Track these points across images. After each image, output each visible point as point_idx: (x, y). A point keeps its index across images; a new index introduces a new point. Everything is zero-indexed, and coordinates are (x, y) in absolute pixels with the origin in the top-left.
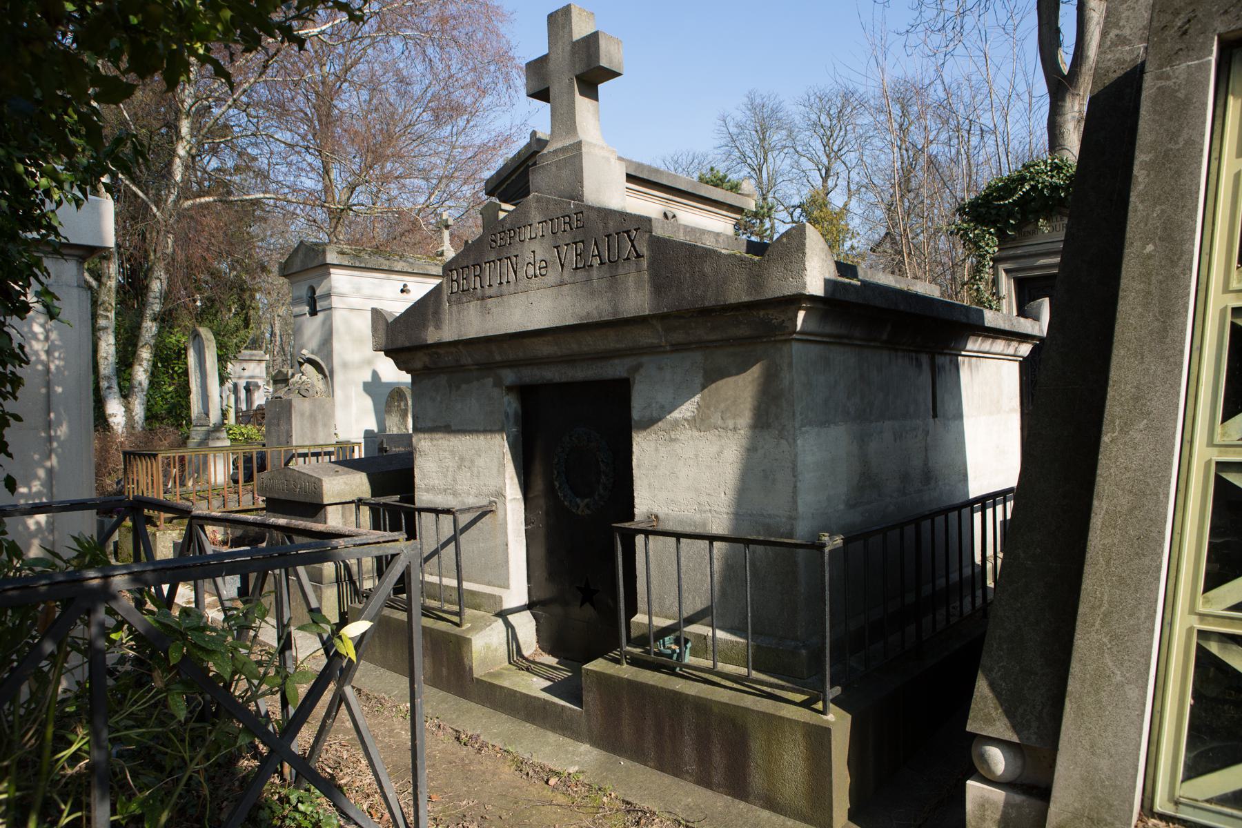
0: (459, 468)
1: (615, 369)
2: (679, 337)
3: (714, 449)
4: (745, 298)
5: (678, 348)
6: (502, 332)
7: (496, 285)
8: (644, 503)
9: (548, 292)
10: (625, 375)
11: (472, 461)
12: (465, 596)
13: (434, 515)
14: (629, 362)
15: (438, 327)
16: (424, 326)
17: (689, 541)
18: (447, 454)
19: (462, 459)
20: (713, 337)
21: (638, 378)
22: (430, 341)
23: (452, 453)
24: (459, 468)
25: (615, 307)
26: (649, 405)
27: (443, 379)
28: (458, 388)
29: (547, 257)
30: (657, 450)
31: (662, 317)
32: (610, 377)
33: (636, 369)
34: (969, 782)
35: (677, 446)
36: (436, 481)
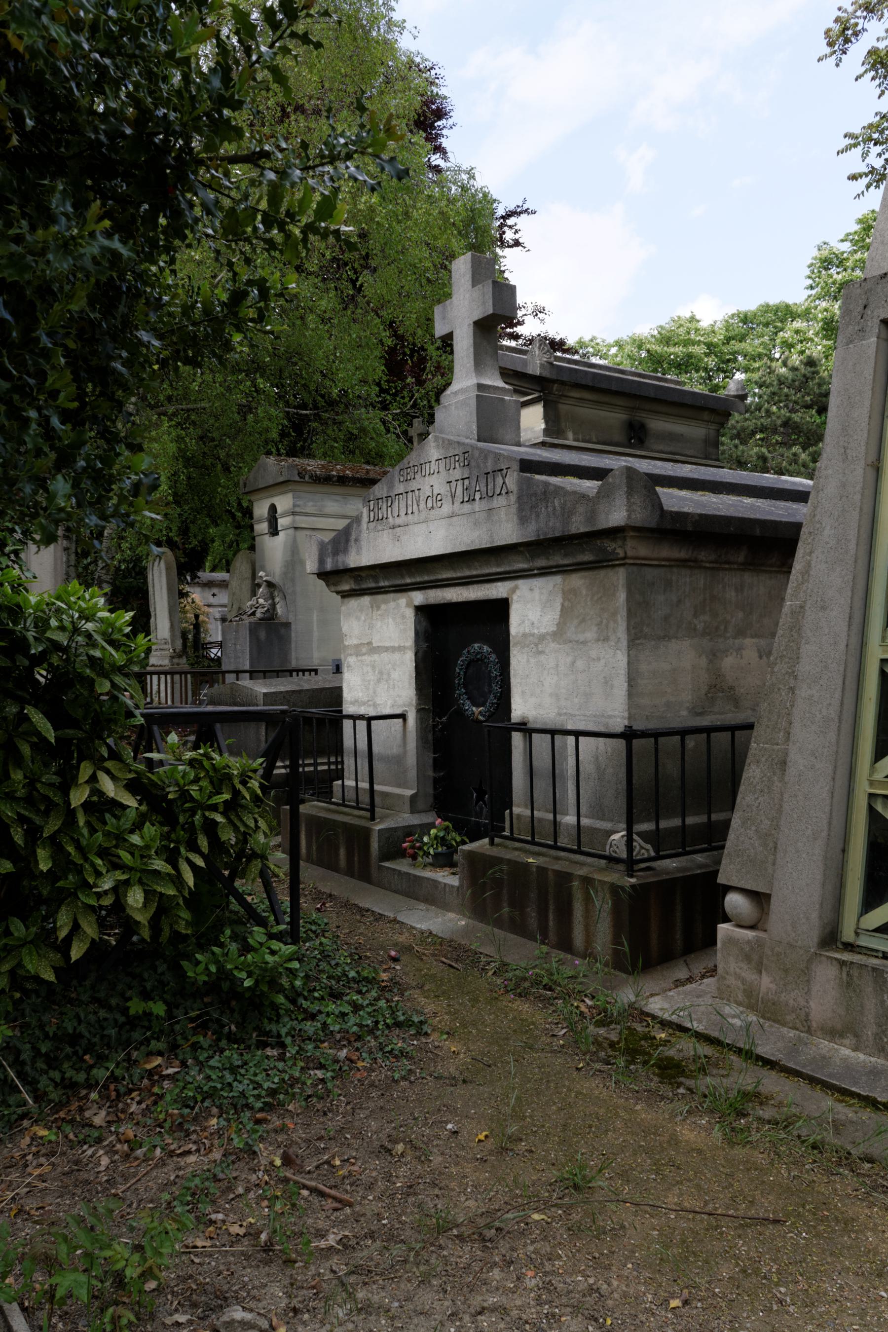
0: (379, 681)
1: (497, 591)
2: (541, 562)
3: (569, 659)
4: (582, 530)
5: (545, 572)
6: (408, 558)
7: (402, 513)
8: (521, 707)
9: (444, 522)
10: (504, 595)
11: (389, 674)
12: (377, 800)
13: (549, 736)
14: (509, 585)
15: (359, 551)
16: (346, 551)
17: (588, 738)
18: (369, 669)
19: (381, 673)
20: (566, 562)
21: (515, 597)
22: (352, 565)
23: (373, 667)
24: (379, 681)
25: (491, 536)
26: (523, 622)
27: (366, 600)
28: (378, 608)
29: (442, 492)
30: (528, 661)
31: (527, 545)
32: (494, 597)
33: (514, 590)
34: (719, 926)
35: (542, 658)
36: (360, 695)
